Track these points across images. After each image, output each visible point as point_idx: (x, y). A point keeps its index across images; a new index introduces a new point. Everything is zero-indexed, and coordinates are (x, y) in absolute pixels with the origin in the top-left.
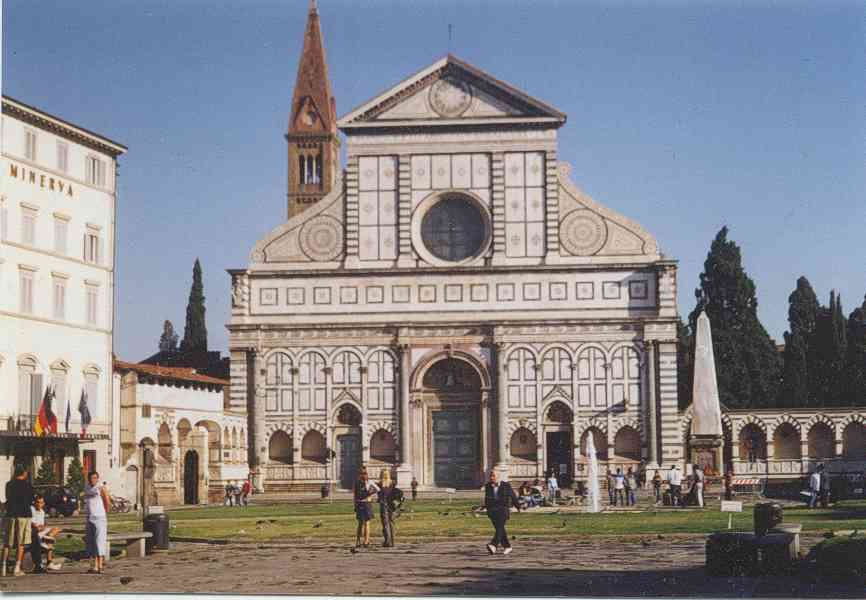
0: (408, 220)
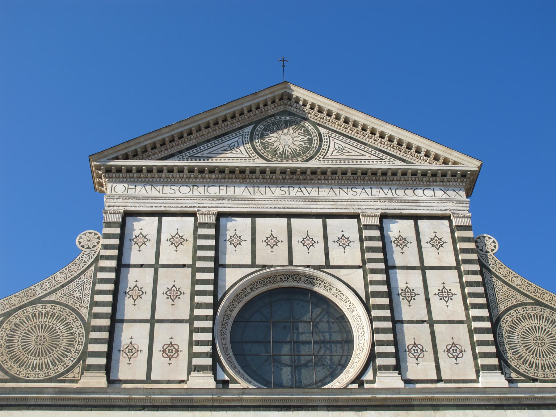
0: (210, 312)
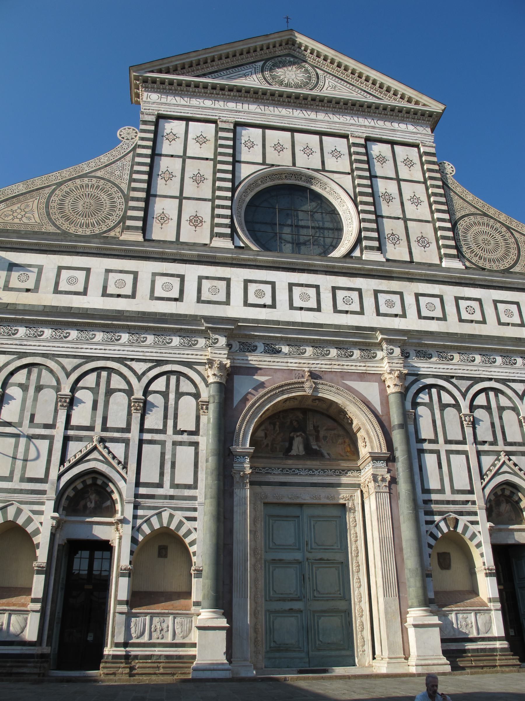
0: (229, 194)
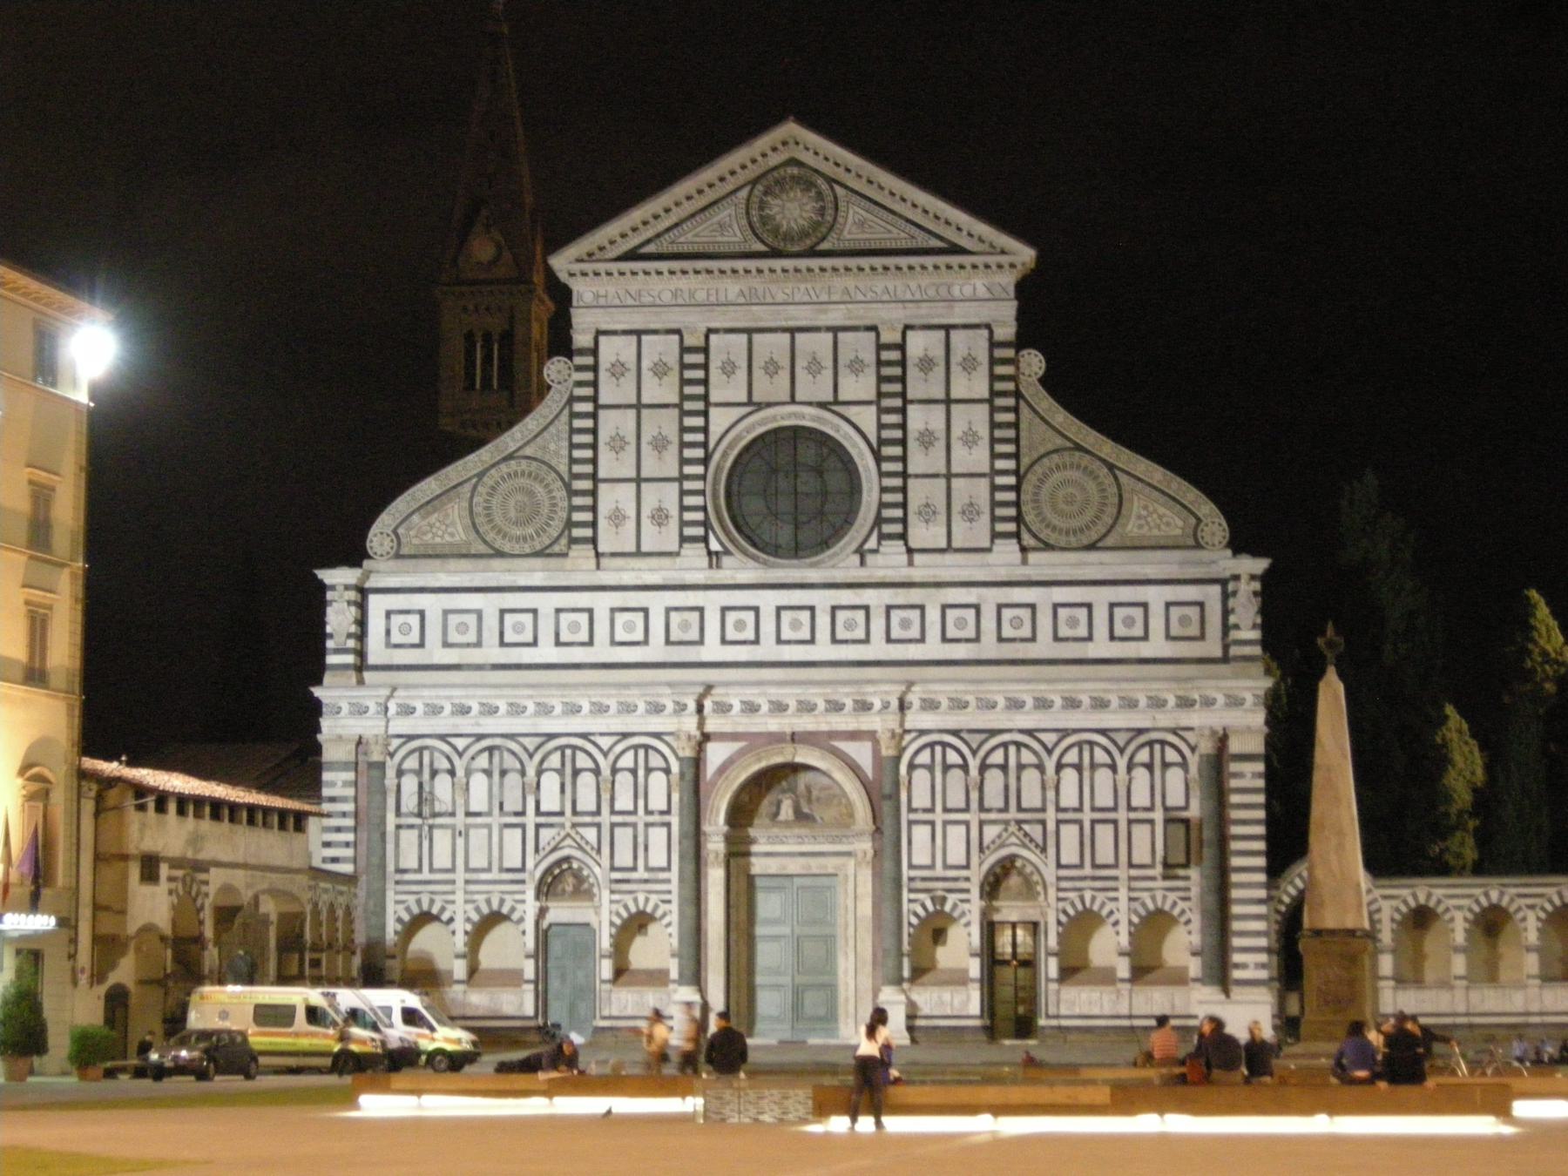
0: (699, 470)
